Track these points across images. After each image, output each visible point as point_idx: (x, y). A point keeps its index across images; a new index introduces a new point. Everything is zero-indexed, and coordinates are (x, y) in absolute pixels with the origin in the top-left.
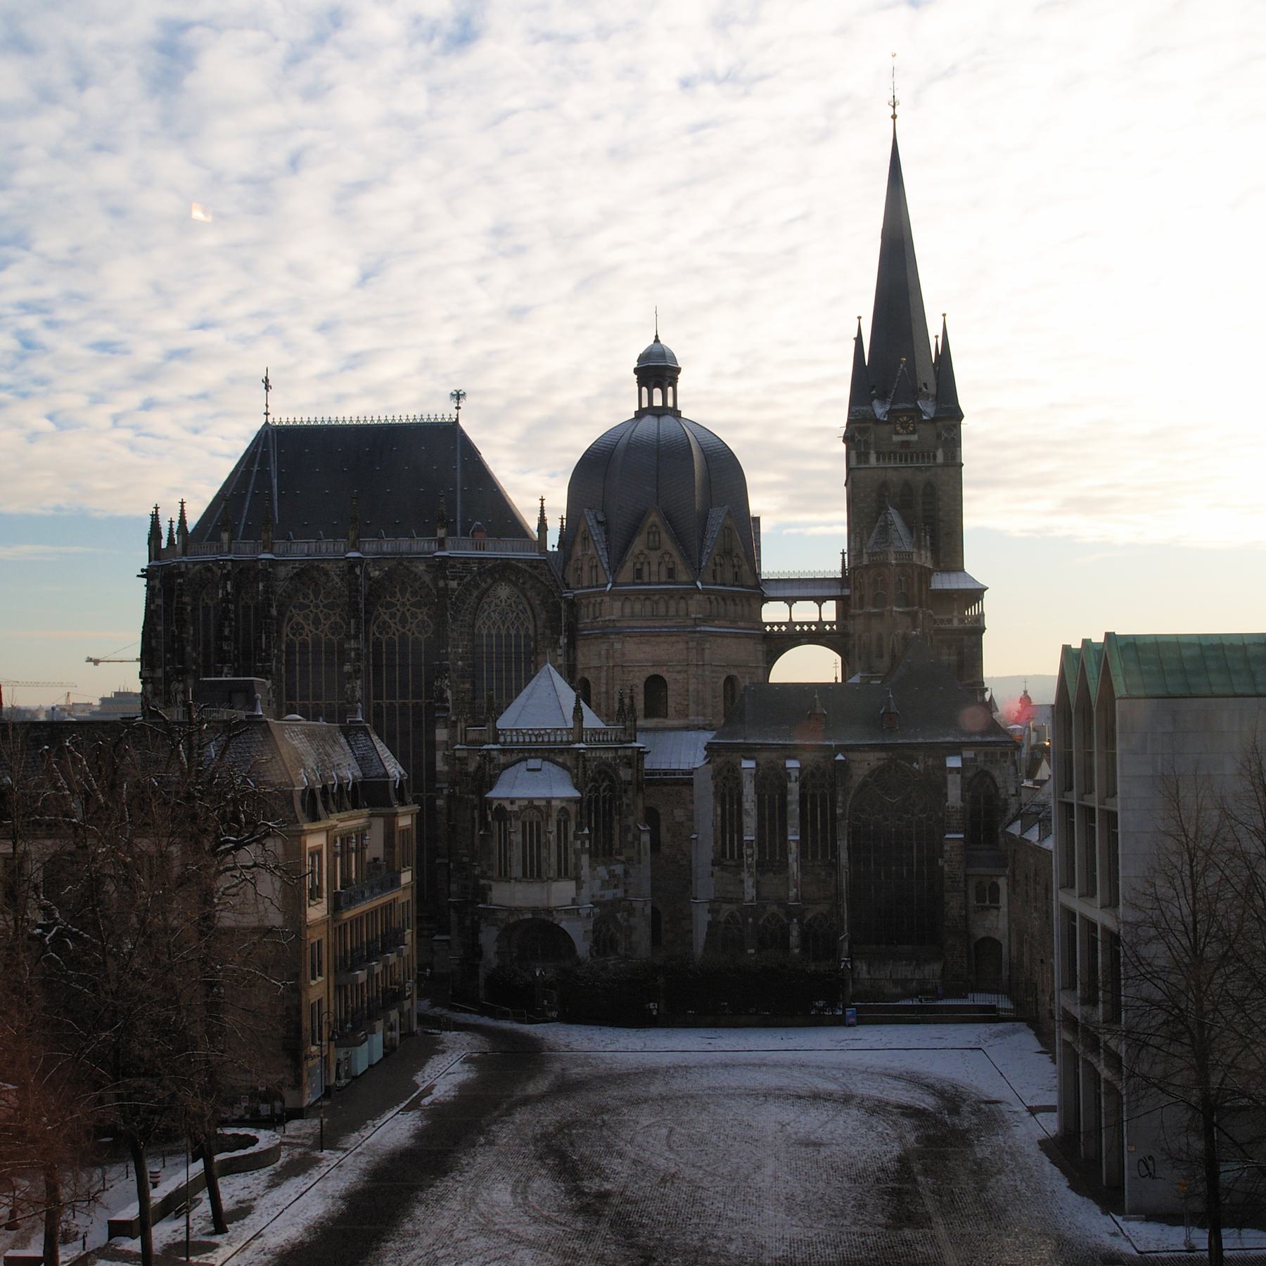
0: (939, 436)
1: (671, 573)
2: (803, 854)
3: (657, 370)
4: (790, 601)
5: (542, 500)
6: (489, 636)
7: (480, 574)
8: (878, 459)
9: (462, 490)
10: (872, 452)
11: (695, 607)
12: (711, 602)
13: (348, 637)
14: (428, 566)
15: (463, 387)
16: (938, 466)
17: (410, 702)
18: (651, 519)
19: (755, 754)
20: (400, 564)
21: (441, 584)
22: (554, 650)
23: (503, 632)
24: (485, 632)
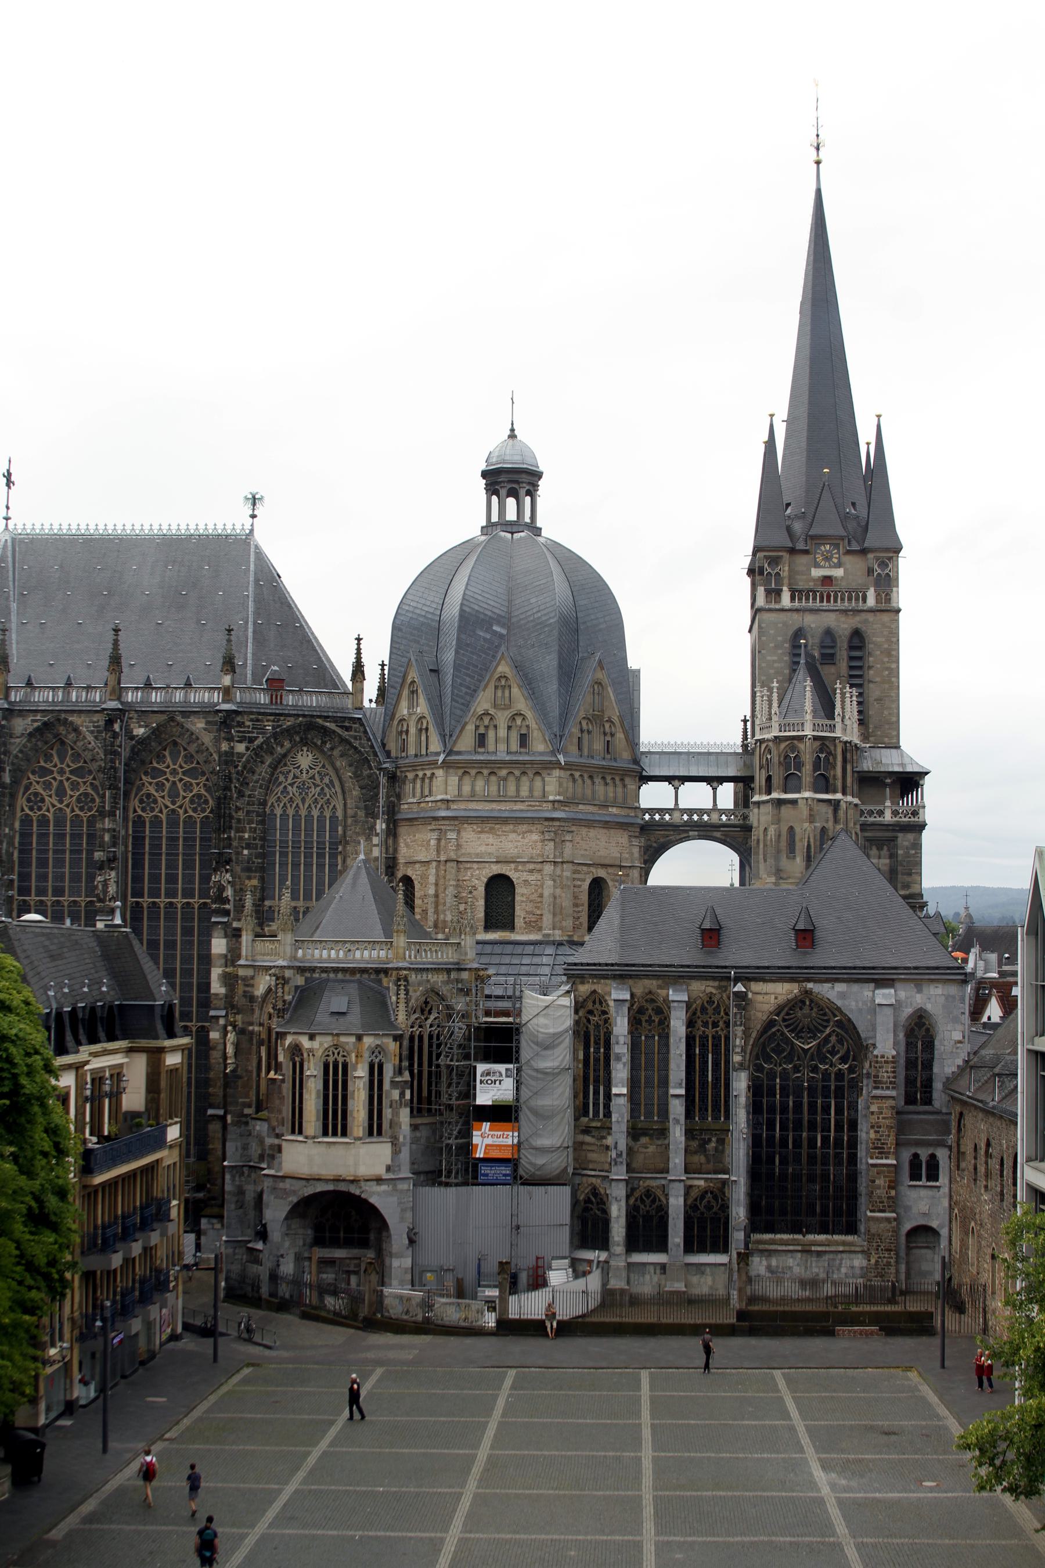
0: (870, 571)
1: (524, 740)
2: (689, 1114)
3: (511, 479)
4: (676, 780)
5: (359, 639)
6: (284, 816)
7: (275, 735)
8: (793, 599)
9: (255, 623)
10: (785, 588)
11: (553, 785)
12: (574, 780)
13: (102, 813)
14: (208, 723)
16: (871, 611)
17: (179, 901)
18: (500, 669)
19: (631, 982)
20: (172, 719)
21: (225, 746)
22: (368, 839)
23: (303, 813)
24: (278, 812)
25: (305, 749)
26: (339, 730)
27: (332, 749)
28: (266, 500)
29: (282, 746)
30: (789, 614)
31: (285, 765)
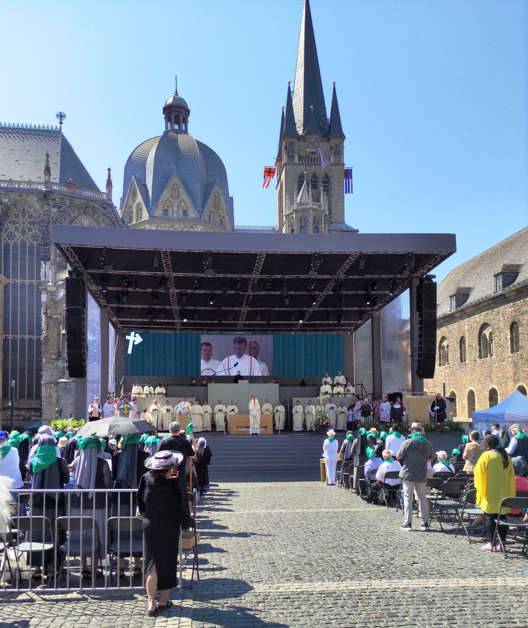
0: (331, 148)
1: (185, 212)
3: (176, 113)
5: (109, 170)
8: (299, 161)
15: (65, 112)
25: (85, 217)
26: (101, 209)
27: (98, 218)
28: (67, 116)
29: (74, 213)
30: (298, 166)
31: (76, 223)
